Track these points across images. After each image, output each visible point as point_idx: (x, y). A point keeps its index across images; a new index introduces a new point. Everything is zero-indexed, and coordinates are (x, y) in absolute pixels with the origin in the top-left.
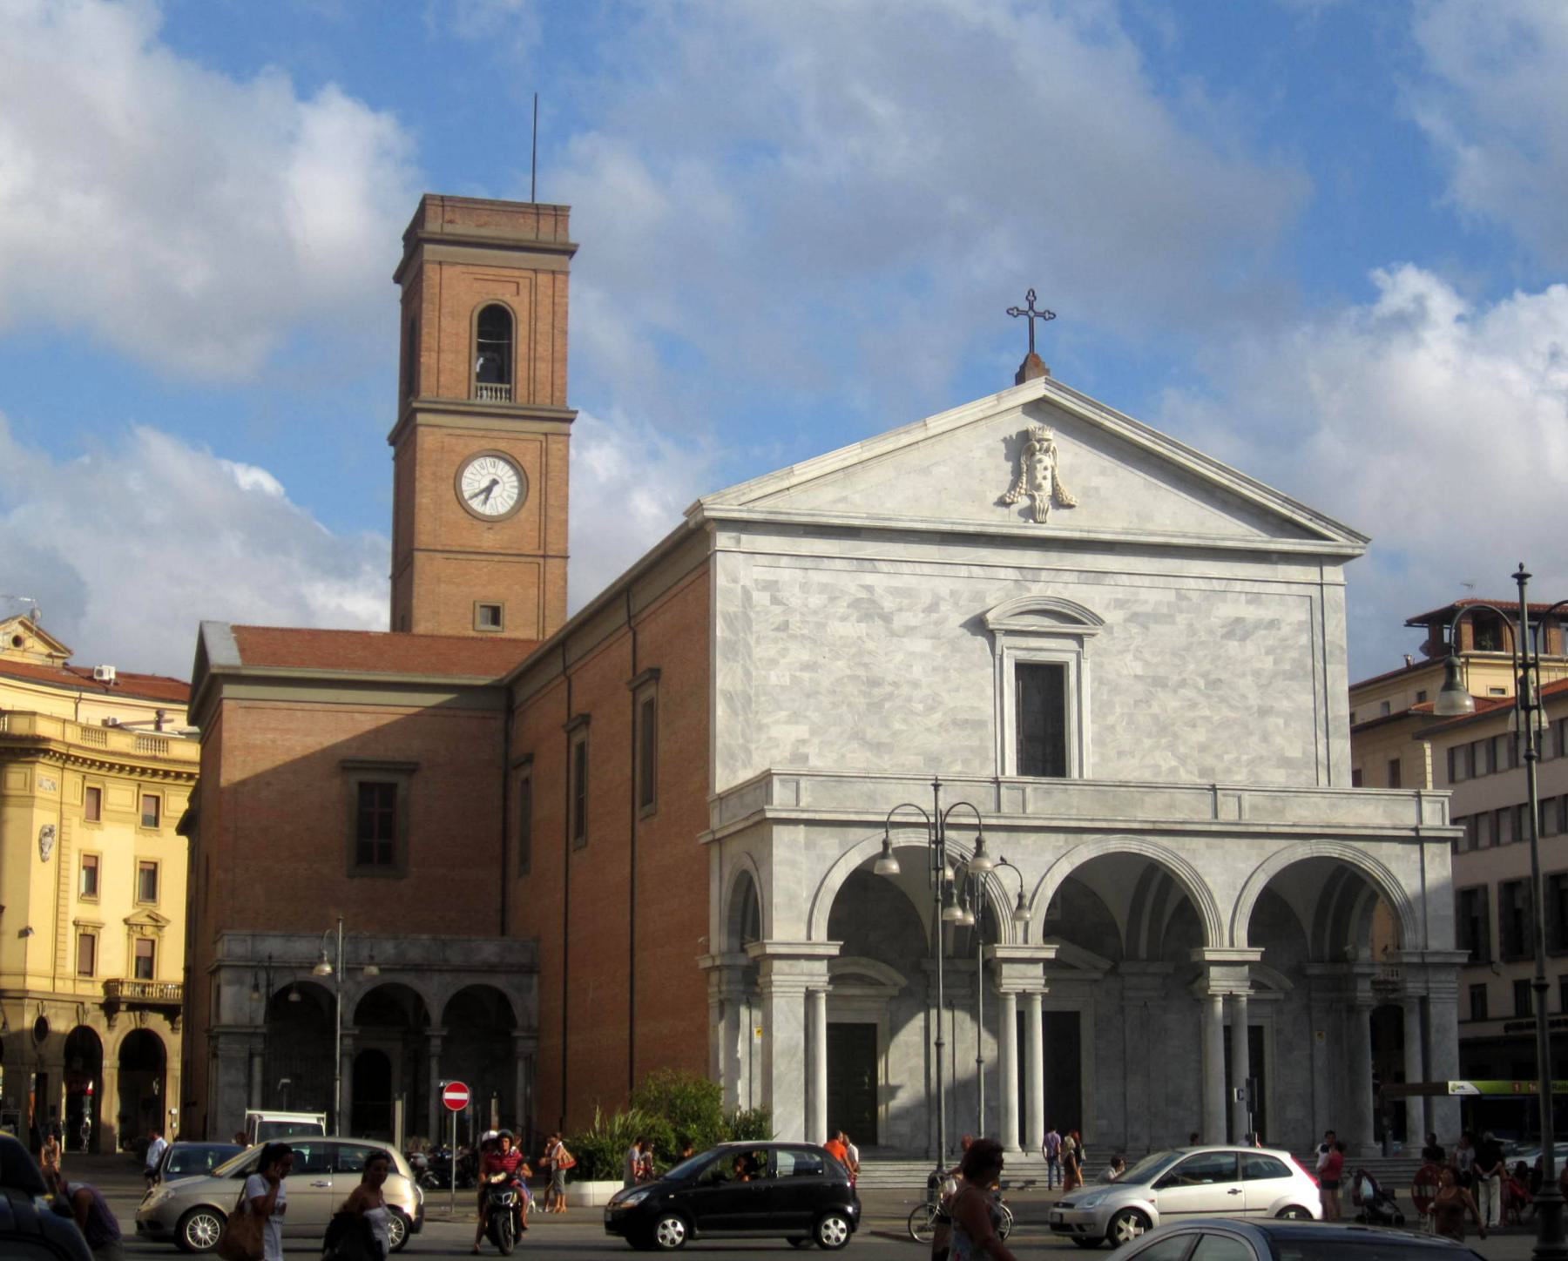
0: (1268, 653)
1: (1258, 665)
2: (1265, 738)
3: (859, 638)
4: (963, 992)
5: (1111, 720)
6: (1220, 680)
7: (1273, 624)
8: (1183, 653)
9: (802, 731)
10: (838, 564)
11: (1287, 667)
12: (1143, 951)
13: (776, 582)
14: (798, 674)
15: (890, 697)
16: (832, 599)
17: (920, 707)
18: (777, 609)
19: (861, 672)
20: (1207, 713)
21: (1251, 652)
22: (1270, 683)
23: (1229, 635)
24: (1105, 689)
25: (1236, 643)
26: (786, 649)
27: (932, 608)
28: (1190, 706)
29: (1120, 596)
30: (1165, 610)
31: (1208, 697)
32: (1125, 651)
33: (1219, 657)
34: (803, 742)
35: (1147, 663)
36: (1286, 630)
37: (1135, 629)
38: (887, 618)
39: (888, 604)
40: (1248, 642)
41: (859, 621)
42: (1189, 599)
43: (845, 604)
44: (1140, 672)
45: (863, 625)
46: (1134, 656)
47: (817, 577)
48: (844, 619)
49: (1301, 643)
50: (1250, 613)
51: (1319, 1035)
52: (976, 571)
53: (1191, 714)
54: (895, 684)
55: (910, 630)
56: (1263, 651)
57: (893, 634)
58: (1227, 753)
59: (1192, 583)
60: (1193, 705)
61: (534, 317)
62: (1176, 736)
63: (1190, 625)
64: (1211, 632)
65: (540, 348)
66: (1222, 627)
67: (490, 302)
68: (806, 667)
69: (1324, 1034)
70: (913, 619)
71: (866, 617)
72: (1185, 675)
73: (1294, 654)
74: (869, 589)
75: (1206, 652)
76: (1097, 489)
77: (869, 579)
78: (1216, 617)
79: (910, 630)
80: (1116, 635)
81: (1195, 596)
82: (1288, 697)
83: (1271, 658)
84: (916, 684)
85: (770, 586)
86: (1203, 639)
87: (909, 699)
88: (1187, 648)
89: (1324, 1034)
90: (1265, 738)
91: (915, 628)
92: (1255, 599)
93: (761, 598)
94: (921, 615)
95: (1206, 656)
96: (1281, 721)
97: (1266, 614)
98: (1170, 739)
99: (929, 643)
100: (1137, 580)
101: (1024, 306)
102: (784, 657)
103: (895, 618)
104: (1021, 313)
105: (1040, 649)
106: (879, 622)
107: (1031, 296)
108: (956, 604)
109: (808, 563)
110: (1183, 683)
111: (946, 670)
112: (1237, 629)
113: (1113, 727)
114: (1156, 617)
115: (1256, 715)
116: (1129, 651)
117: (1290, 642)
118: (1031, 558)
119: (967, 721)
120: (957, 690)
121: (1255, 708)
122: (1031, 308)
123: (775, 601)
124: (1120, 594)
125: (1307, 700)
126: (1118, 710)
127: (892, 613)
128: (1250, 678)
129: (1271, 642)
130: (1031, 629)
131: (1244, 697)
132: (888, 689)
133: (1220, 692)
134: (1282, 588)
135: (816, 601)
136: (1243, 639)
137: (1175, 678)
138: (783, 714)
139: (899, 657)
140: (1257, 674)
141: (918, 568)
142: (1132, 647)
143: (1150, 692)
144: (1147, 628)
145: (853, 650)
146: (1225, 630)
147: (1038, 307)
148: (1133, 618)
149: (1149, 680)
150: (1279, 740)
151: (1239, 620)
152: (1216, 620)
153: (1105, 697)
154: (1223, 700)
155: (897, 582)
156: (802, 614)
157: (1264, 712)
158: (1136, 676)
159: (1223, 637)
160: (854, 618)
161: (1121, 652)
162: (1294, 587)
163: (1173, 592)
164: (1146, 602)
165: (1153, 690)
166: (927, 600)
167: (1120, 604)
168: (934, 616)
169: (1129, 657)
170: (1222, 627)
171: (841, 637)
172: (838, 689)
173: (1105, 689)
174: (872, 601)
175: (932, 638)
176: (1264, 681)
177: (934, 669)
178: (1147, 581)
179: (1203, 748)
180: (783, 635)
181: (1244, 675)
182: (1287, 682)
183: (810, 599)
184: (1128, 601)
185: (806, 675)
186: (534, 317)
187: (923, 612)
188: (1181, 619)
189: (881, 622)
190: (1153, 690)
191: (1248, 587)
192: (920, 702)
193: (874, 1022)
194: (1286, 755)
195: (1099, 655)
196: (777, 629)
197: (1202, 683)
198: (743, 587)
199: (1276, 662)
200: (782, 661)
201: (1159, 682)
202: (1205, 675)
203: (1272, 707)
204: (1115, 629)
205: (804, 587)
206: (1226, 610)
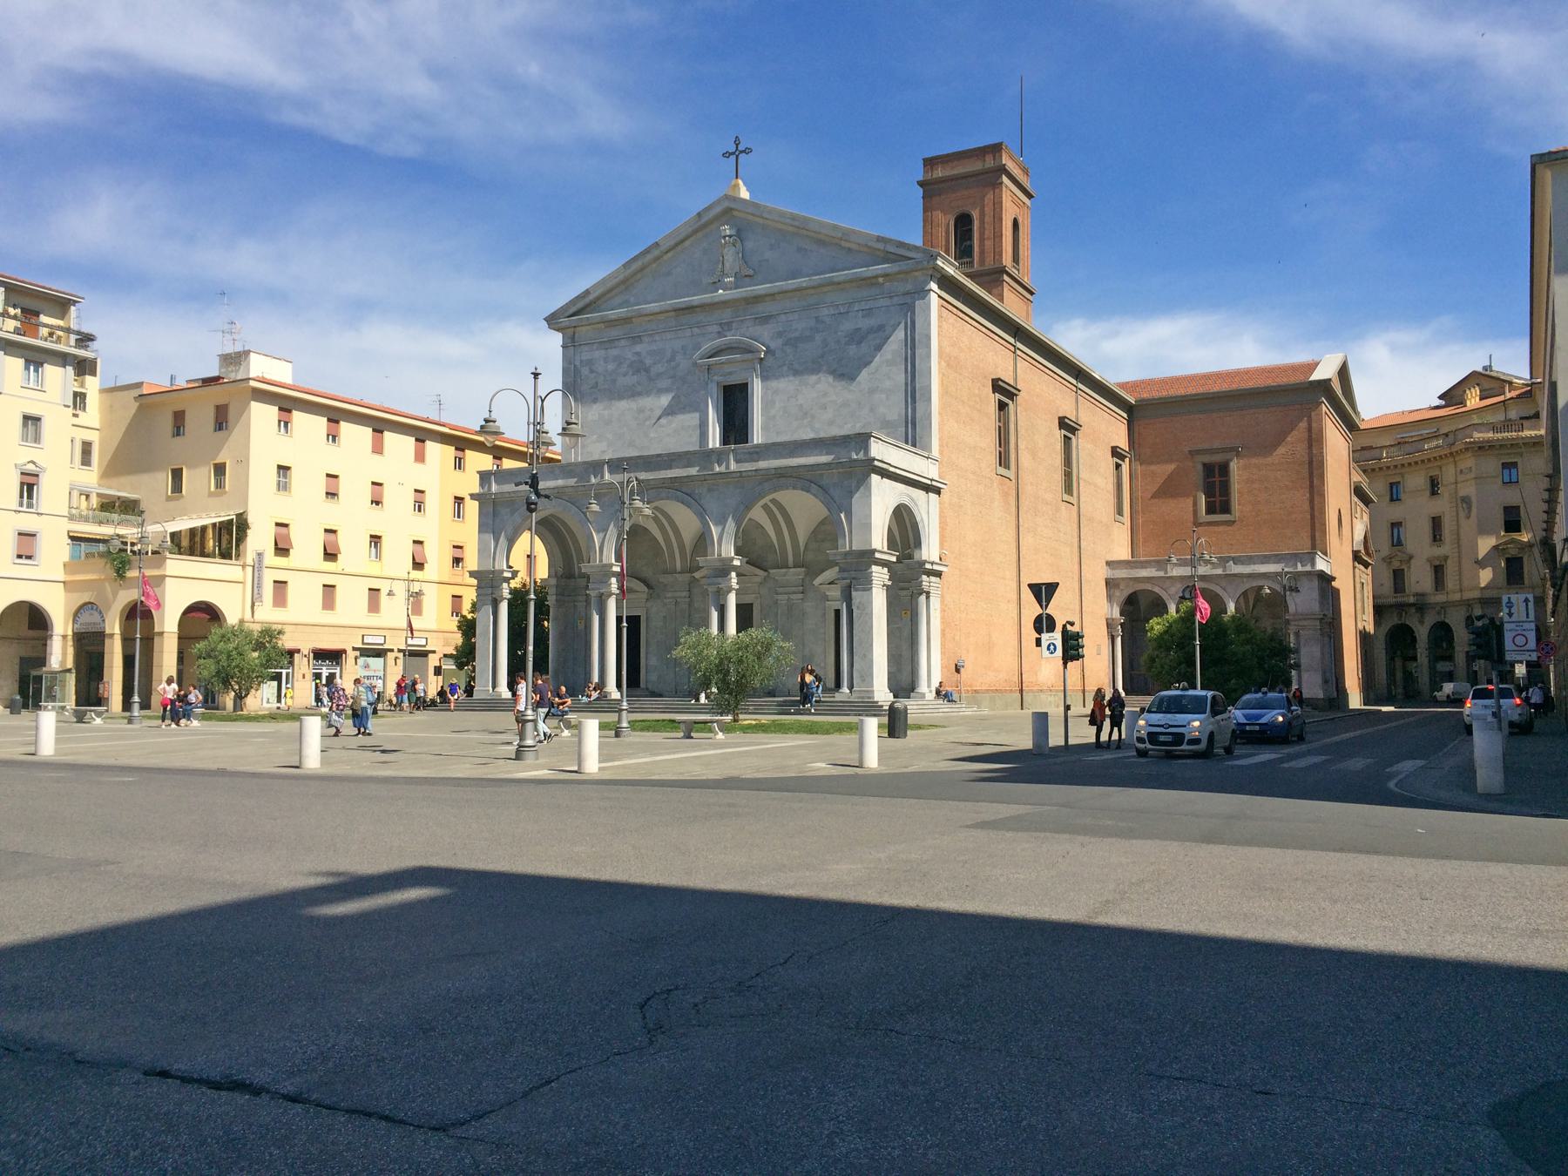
3: (633, 385)
4: (684, 594)
5: (773, 412)
8: (820, 360)
10: (623, 343)
16: (621, 363)
18: (593, 375)
27: (672, 359)
29: (781, 329)
34: (604, 452)
37: (789, 350)
38: (647, 370)
39: (648, 362)
40: (863, 345)
41: (633, 375)
43: (626, 366)
45: (635, 377)
47: (614, 352)
55: (659, 375)
56: (873, 348)
58: (846, 424)
61: (982, 215)
62: (813, 417)
65: (987, 232)
66: (845, 337)
70: (659, 368)
74: (638, 354)
77: (638, 348)
85: (590, 363)
88: (822, 356)
90: (872, 410)
92: (869, 313)
93: (585, 371)
94: (666, 365)
95: (834, 359)
96: (884, 396)
98: (809, 419)
99: (670, 380)
101: (741, 148)
103: (652, 369)
105: (730, 373)
107: (737, 142)
108: (685, 354)
113: (774, 417)
116: (785, 365)
119: (689, 426)
121: (866, 390)
122: (741, 152)
123: (592, 371)
125: (901, 378)
126: (777, 405)
127: (650, 367)
135: (611, 367)
136: (859, 343)
143: (797, 390)
144: (796, 347)
146: (847, 339)
147: (741, 148)
150: (882, 410)
153: (770, 398)
155: (654, 347)
156: (604, 376)
159: (846, 344)
160: (631, 373)
161: (780, 367)
162: (896, 299)
164: (796, 330)
165: (799, 388)
169: (785, 368)
170: (845, 337)
174: (641, 362)
175: (671, 378)
176: (873, 371)
178: (796, 316)
179: (831, 423)
183: (609, 367)
186: (982, 215)
187: (667, 362)
188: (818, 338)
189: (644, 373)
190: (799, 388)
191: (864, 306)
195: (767, 371)
198: (575, 366)
205: (606, 360)
206: (847, 326)
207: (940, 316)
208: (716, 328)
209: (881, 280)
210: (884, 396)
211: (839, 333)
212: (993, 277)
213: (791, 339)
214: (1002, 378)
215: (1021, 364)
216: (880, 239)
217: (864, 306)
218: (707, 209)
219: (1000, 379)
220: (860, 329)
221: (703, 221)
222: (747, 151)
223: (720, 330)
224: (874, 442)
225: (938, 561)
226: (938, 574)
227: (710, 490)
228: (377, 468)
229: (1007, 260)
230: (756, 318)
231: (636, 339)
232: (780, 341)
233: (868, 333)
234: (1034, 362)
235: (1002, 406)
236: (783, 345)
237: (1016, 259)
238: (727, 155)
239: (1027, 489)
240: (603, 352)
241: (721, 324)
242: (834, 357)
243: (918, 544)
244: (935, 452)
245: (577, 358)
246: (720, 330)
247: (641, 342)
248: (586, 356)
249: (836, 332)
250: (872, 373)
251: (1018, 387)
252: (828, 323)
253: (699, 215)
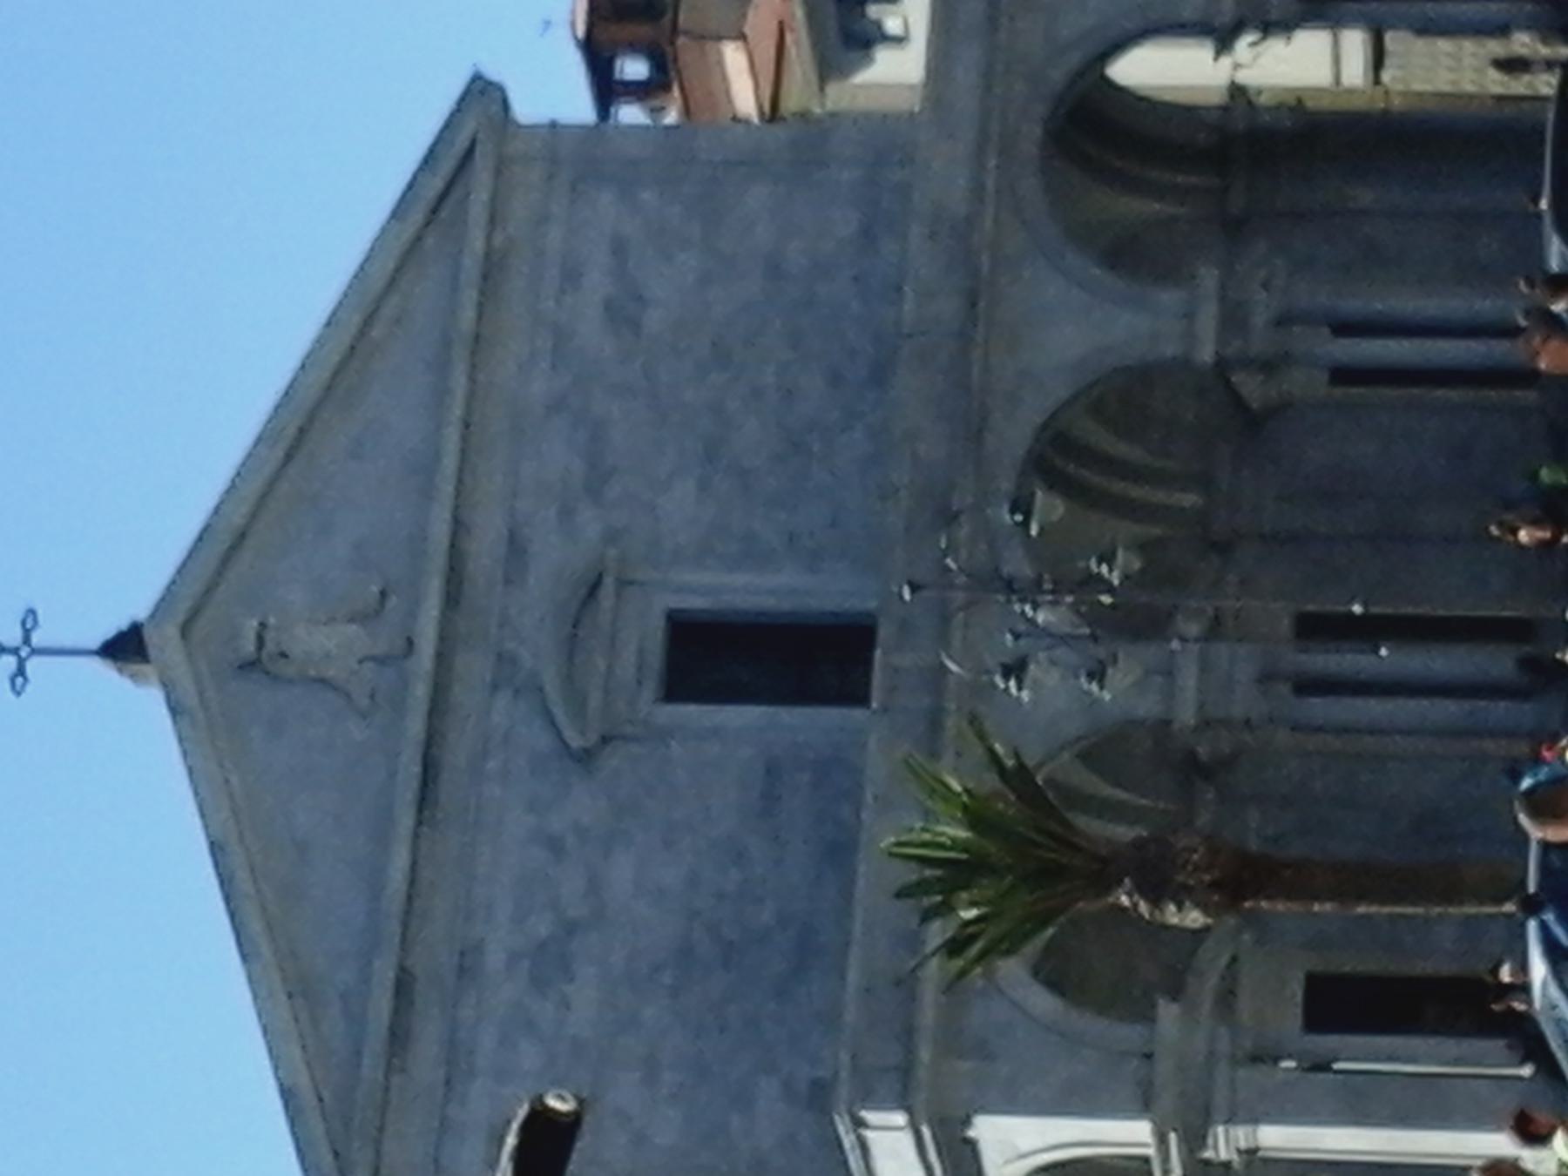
7: (619, 248)
9: (768, 1089)
12: (1189, 499)
19: (667, 978)
23: (635, 326)
27: (555, 846)
39: (542, 927)
48: (565, 1004)
50: (597, 284)
55: (594, 886)
74: (513, 958)
77: (495, 958)
79: (594, 886)
92: (571, 276)
104: (21, 671)
105: (641, 652)
125: (758, 197)
136: (640, 299)
138: (736, 1121)
151: (610, 308)
167: (567, 514)
193: (1301, 976)
206: (590, 330)
209: (498, 240)
231: (467, 966)
247: (479, 947)
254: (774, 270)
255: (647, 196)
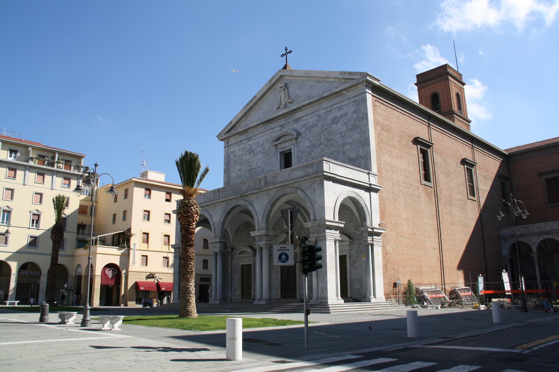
0: (344, 125)
1: (341, 130)
2: (344, 154)
3: (249, 159)
6: (331, 139)
7: (346, 114)
8: (320, 134)
10: (245, 141)
11: (350, 127)
13: (234, 151)
14: (237, 173)
15: (254, 172)
16: (244, 150)
17: (260, 173)
20: (327, 151)
21: (340, 127)
22: (345, 134)
23: (332, 124)
24: (300, 153)
25: (335, 125)
26: (236, 167)
28: (322, 150)
29: (304, 123)
30: (315, 123)
31: (327, 146)
32: (305, 140)
33: (330, 131)
35: (311, 141)
36: (349, 115)
37: (307, 132)
38: (254, 152)
39: (254, 148)
40: (338, 124)
41: (249, 154)
42: (321, 117)
43: (246, 151)
44: (309, 145)
45: (249, 155)
46: (308, 140)
48: (246, 155)
49: (354, 117)
50: (338, 114)
51: (363, 256)
52: (271, 131)
53: (323, 153)
54: (255, 169)
56: (343, 125)
57: (255, 155)
59: (322, 111)
60: (323, 150)
63: (322, 126)
64: (328, 124)
67: (434, 92)
68: (240, 170)
69: (365, 256)
70: (258, 150)
71: (250, 153)
72: (321, 141)
73: (352, 122)
74: (250, 145)
75: (327, 131)
76: (298, 94)
77: (250, 142)
78: (329, 119)
80: (303, 136)
81: (323, 115)
82: (351, 137)
83: (345, 126)
84: (259, 167)
85: (234, 152)
86: (326, 127)
87: (258, 172)
88: (321, 133)
89: (365, 256)
90: (344, 154)
91: (259, 152)
92: (340, 108)
93: (232, 156)
95: (326, 133)
96: (349, 146)
97: (342, 112)
99: (262, 155)
100: (308, 117)
102: (235, 169)
103: (255, 151)
105: (285, 147)
106: (252, 153)
107: (286, 49)
108: (267, 142)
109: (240, 143)
110: (320, 144)
111: (265, 161)
112: (336, 121)
114: (313, 126)
115: (341, 147)
117: (351, 119)
118: (282, 122)
120: (267, 166)
121: (341, 145)
123: (234, 156)
124: (304, 123)
126: (304, 158)
127: (255, 150)
128: (339, 135)
129: (345, 121)
130: (280, 142)
131: (337, 142)
132: (254, 170)
133: (331, 143)
134: (347, 102)
135: (241, 153)
136: (337, 123)
137: (319, 143)
139: (256, 161)
140: (341, 133)
141: (259, 136)
142: (307, 138)
143: (312, 150)
144: (311, 130)
145: (247, 163)
148: (307, 129)
149: (311, 146)
150: (348, 153)
151: (336, 117)
152: (329, 120)
153: (301, 155)
154: (332, 145)
155: (256, 141)
157: (344, 145)
158: (308, 146)
159: (331, 125)
160: (248, 154)
161: (304, 140)
162: (351, 100)
163: (317, 116)
164: (310, 122)
165: (312, 149)
166: (261, 143)
167: (304, 126)
168: (263, 146)
171: (245, 160)
172: (244, 174)
173: (300, 153)
174: (251, 148)
175: (262, 153)
176: (343, 135)
177: (263, 161)
178: (310, 116)
180: (235, 164)
181: (338, 135)
182: (350, 132)
184: (306, 124)
185: (239, 172)
188: (320, 124)
191: (338, 105)
192: (260, 172)
194: (351, 157)
196: (234, 163)
197: (325, 142)
198: (228, 154)
199: (347, 127)
200: (235, 170)
201: (314, 146)
202: (326, 139)
203: (346, 142)
204: (303, 133)
205: (239, 150)
206: (331, 116)
207: (374, 105)
208: (279, 128)
210: (349, 146)
211: (328, 120)
212: (450, 113)
213: (308, 127)
214: (419, 137)
215: (433, 132)
216: (341, 73)
217: (338, 105)
218: (273, 78)
219: (418, 138)
220: (337, 117)
221: (272, 83)
222: (290, 52)
223: (281, 128)
224: (371, 176)
225: (378, 227)
226: (378, 234)
227: (256, 198)
228: (147, 204)
229: (455, 108)
230: (294, 120)
231: (249, 139)
232: (304, 129)
233: (341, 118)
234: (443, 132)
235: (424, 153)
236: (305, 130)
237: (460, 108)
238: (282, 56)
239: (444, 194)
240: (238, 146)
241: (280, 126)
242: (327, 131)
243: (364, 219)
244: (374, 169)
245: (229, 151)
246: (281, 128)
248: (232, 150)
249: (327, 120)
250: (343, 136)
251: (432, 142)
252: (323, 116)
253: (270, 81)
254: (344, 145)
255: (355, 116)
